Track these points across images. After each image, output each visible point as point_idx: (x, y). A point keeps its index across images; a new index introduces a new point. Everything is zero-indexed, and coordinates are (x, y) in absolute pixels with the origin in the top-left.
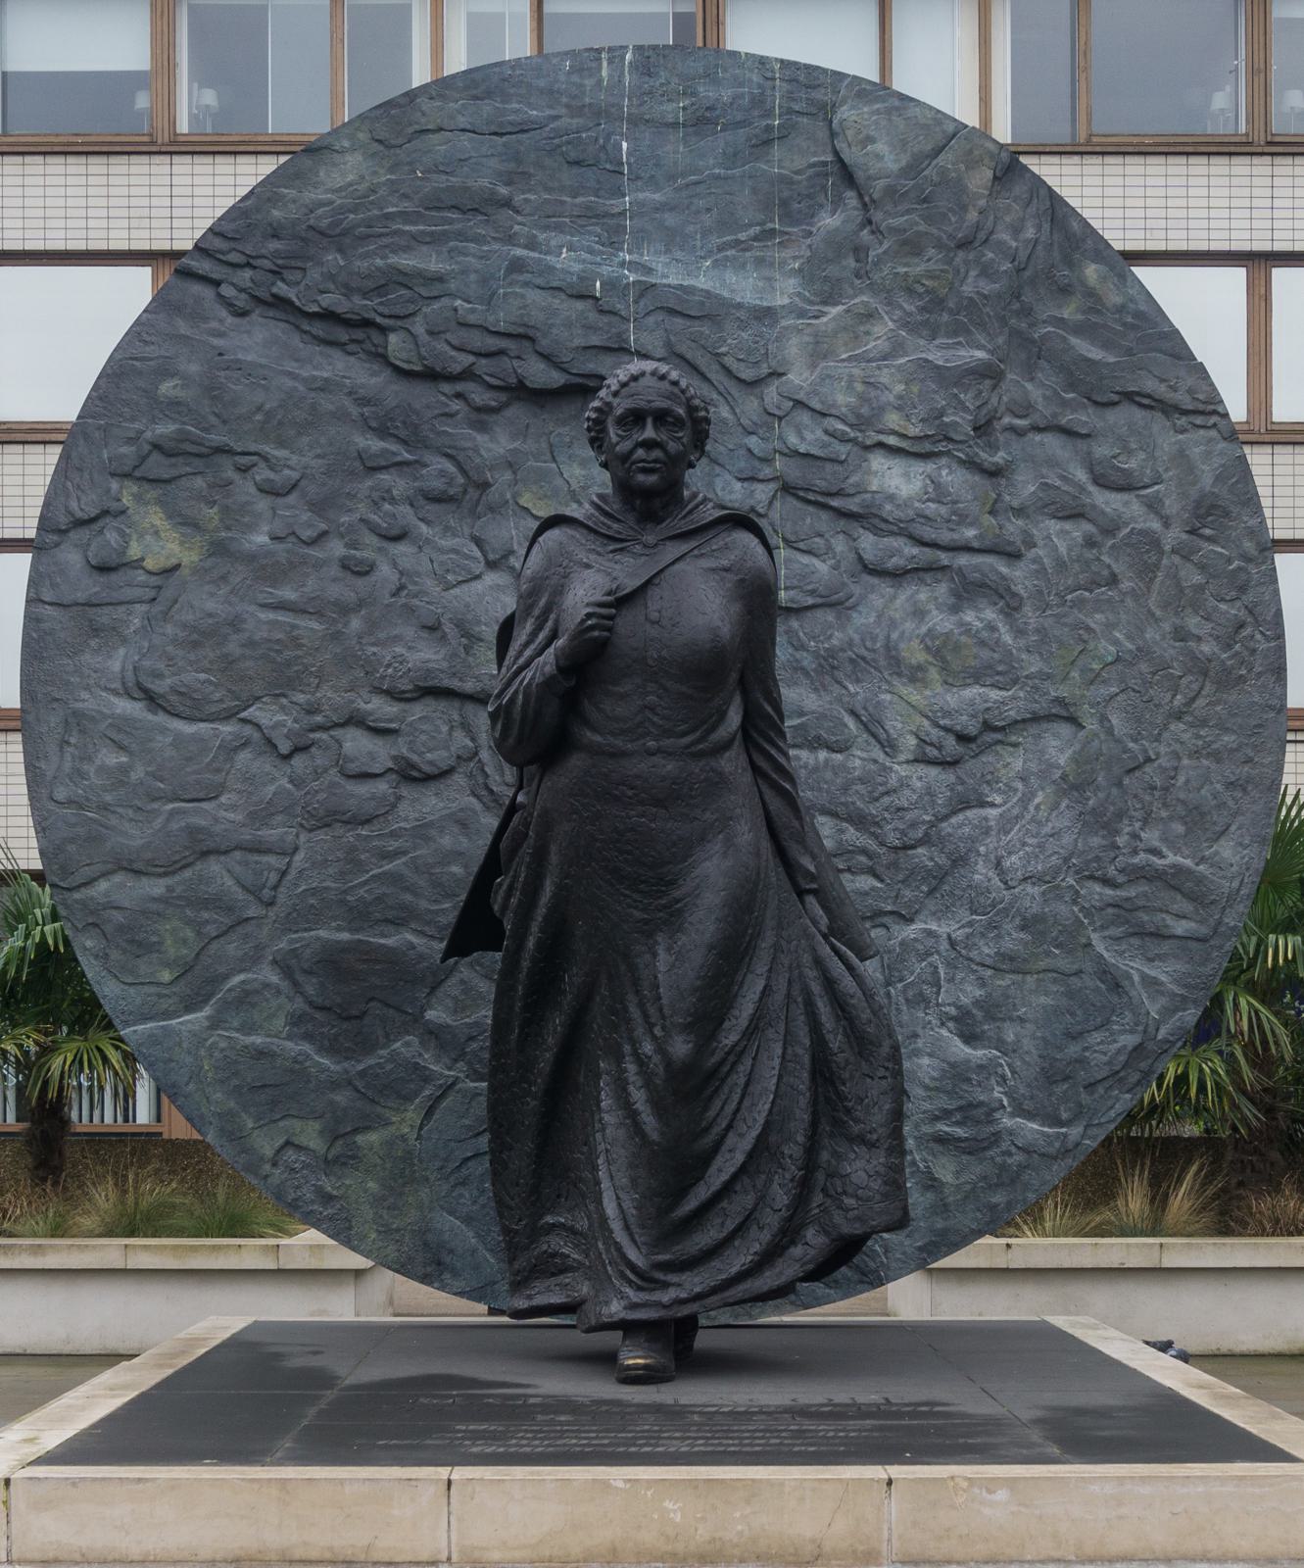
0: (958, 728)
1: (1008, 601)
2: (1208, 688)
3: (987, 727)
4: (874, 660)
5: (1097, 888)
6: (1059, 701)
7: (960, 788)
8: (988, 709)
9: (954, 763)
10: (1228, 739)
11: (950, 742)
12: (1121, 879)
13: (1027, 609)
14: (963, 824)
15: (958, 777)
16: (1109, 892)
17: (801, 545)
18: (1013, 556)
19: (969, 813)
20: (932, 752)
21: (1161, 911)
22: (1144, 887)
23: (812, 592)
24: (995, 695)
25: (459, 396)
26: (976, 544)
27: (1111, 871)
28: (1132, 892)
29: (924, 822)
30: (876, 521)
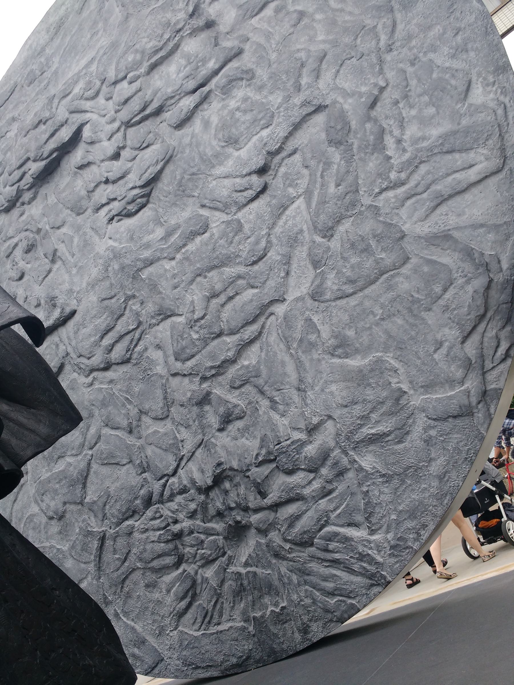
0: (254, 168)
1: (248, 76)
2: (398, 16)
3: (272, 154)
4: (199, 170)
5: (390, 194)
6: (306, 103)
7: (274, 201)
8: (266, 144)
9: (264, 189)
10: (437, 29)
11: (255, 178)
12: (403, 175)
13: (259, 72)
14: (287, 221)
15: (271, 196)
16: (401, 191)
17: (144, 145)
18: (239, 53)
19: (287, 212)
20: (250, 193)
21: (448, 175)
22: (423, 169)
23: (157, 162)
24: (265, 133)
25: (23, 204)
26: (217, 66)
27: (393, 175)
28: (416, 178)
29: (263, 236)
30: (170, 102)
